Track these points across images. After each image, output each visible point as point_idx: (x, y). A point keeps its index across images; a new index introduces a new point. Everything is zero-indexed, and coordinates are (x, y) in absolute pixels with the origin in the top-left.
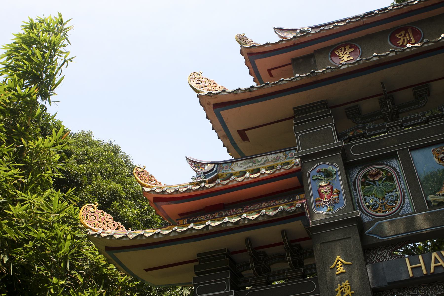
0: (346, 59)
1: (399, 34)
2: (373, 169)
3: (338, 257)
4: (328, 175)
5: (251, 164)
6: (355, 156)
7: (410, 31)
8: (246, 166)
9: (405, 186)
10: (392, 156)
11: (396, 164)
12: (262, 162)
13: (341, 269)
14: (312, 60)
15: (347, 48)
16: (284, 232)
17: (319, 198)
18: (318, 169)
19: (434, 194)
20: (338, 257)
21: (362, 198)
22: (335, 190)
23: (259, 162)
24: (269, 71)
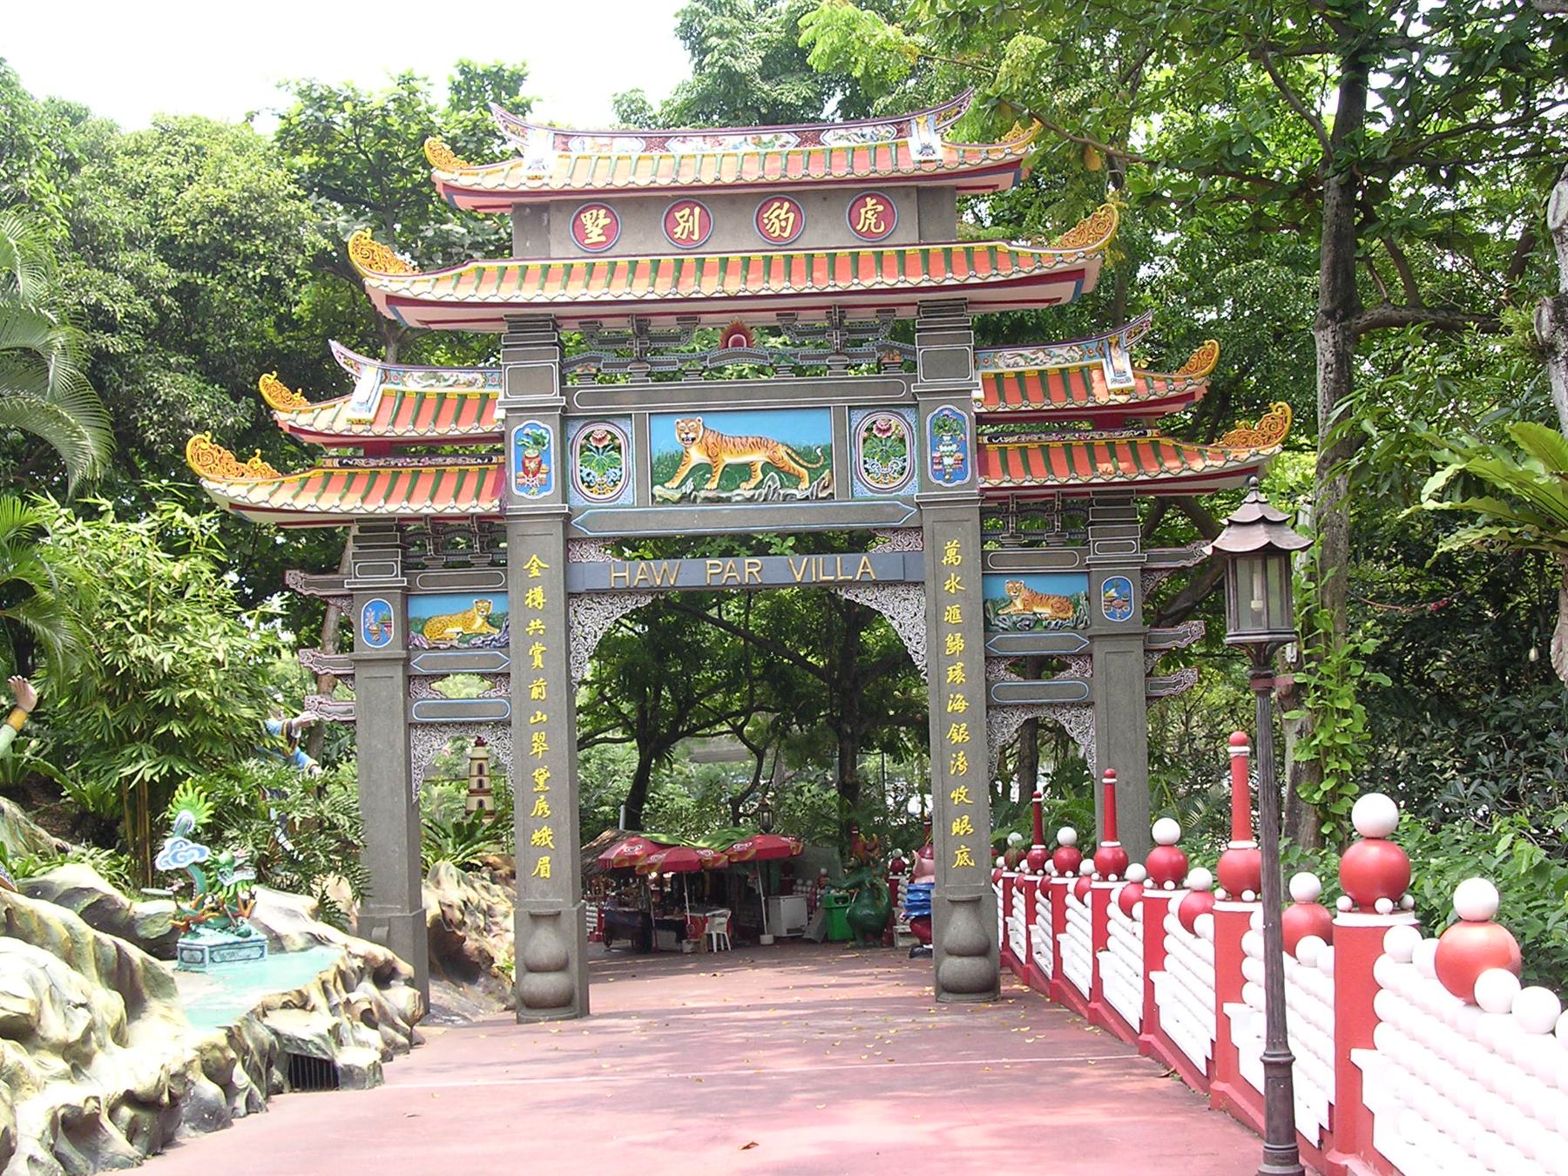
0: (595, 239)
1: (681, 214)
2: (600, 429)
3: (534, 557)
4: (538, 442)
5: (433, 381)
6: (581, 409)
7: (697, 210)
8: (425, 383)
9: (632, 464)
11: (628, 427)
12: (450, 382)
13: (535, 572)
14: (545, 217)
15: (602, 212)
17: (522, 474)
18: (527, 430)
19: (663, 485)
20: (534, 557)
21: (579, 468)
22: (544, 466)
23: (446, 380)
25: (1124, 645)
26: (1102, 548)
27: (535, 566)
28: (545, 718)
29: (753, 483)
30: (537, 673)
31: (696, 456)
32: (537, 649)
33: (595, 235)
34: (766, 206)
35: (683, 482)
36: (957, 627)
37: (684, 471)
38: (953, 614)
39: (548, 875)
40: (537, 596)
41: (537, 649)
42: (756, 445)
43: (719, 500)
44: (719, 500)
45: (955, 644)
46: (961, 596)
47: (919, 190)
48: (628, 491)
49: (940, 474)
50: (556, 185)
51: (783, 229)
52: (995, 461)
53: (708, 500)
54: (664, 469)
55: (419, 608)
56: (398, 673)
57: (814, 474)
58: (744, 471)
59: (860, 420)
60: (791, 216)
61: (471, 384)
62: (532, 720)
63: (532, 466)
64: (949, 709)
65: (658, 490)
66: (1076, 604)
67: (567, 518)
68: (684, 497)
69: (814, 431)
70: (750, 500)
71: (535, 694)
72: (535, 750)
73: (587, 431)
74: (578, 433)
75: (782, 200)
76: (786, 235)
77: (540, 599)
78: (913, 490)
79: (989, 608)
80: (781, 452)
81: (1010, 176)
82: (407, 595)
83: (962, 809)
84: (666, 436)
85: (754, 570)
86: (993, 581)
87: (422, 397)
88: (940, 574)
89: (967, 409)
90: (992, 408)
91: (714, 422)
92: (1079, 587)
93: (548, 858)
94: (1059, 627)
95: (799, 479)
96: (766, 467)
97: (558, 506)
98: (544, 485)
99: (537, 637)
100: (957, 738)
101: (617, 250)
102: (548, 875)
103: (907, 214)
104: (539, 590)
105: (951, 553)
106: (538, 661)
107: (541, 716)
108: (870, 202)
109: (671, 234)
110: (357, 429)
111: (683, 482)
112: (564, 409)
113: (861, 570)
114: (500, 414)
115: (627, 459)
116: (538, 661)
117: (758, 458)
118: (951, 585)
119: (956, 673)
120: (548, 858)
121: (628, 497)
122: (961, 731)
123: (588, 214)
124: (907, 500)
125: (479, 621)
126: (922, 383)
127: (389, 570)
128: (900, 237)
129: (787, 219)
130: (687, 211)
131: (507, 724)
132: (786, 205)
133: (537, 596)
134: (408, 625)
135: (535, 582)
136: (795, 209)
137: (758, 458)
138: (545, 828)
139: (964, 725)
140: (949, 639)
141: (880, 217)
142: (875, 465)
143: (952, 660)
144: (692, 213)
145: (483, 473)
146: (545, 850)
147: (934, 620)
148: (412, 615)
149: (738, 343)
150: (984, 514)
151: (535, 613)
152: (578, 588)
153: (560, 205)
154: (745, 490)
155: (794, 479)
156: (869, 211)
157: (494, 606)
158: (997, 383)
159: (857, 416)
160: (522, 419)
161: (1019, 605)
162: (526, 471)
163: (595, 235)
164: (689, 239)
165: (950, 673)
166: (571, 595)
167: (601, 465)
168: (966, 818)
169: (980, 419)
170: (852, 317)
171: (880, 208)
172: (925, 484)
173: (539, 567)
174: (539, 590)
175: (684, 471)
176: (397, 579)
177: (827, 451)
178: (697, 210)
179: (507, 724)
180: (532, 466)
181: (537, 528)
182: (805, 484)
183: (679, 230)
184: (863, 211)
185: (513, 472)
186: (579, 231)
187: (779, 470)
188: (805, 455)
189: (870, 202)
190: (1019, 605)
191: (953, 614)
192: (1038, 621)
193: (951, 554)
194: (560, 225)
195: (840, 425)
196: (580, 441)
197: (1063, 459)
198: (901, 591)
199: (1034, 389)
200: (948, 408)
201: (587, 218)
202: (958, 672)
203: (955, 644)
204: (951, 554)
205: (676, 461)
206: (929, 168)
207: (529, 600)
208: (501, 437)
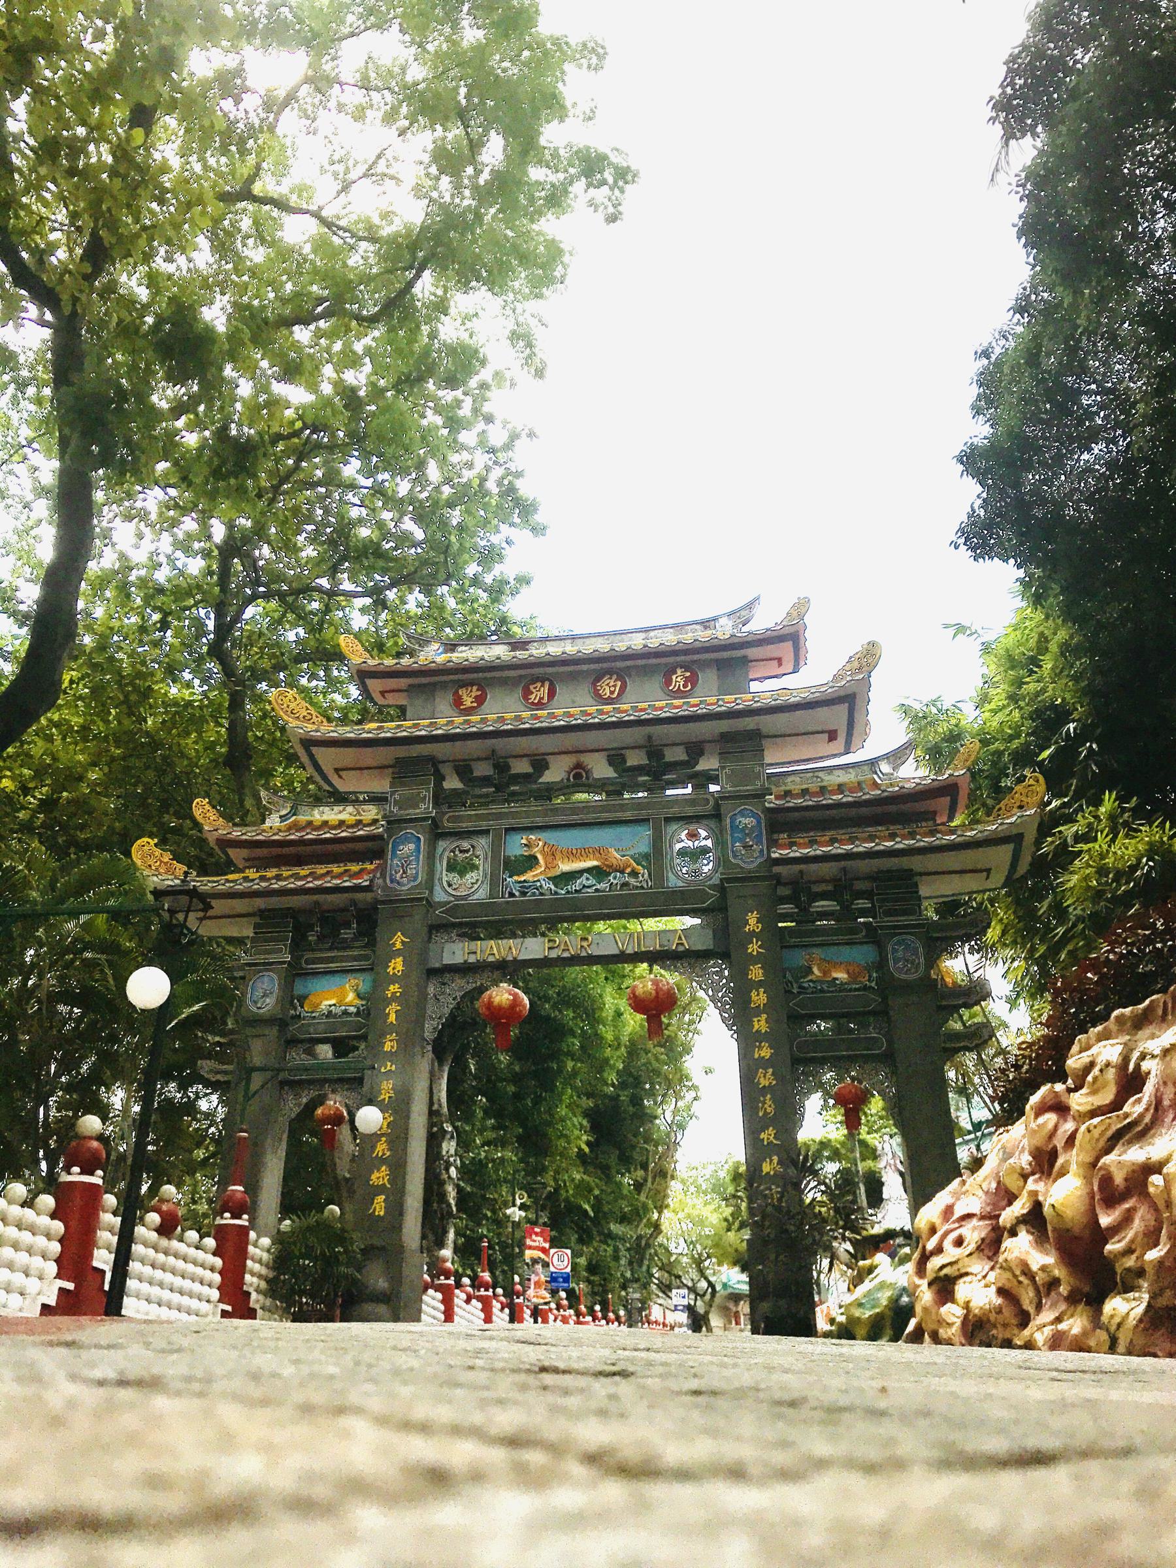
7: (547, 685)
10: (487, 832)
13: (399, 946)
15: (475, 688)
16: (354, 902)
24: (383, 693)
27: (398, 941)
28: (393, 1068)
30: (392, 1028)
34: (598, 679)
36: (760, 984)
38: (756, 973)
39: (382, 1213)
40: (397, 965)
47: (717, 660)
51: (612, 692)
56: (273, 1032)
60: (619, 683)
62: (383, 1070)
64: (756, 1056)
71: (387, 1047)
72: (382, 1097)
76: (615, 695)
77: (400, 968)
85: (585, 944)
93: (384, 1197)
99: (394, 998)
100: (764, 1082)
102: (382, 1213)
104: (400, 960)
106: (392, 1018)
112: (435, 823)
113: (676, 941)
116: (392, 1018)
118: (754, 948)
120: (384, 1197)
122: (768, 1075)
123: (464, 690)
129: (615, 686)
130: (539, 684)
132: (615, 677)
133: (397, 965)
138: (383, 1168)
139: (770, 1070)
140: (753, 994)
141: (687, 680)
143: (758, 1012)
144: (543, 686)
146: (380, 1190)
148: (296, 993)
151: (394, 979)
153: (444, 686)
156: (678, 680)
163: (468, 701)
165: (756, 1024)
168: (775, 1158)
171: (688, 674)
173: (403, 942)
174: (400, 960)
178: (547, 685)
183: (533, 696)
184: (674, 677)
186: (458, 702)
189: (679, 671)
202: (763, 1023)
204: (753, 922)
207: (390, 970)
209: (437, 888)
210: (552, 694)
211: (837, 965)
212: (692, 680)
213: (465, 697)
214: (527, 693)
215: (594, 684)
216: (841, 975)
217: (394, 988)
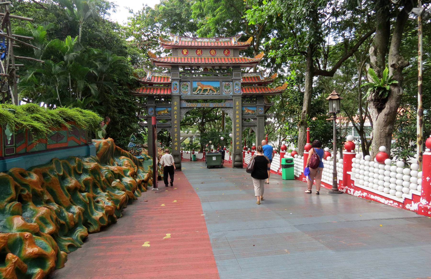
2: (185, 83)
4: (176, 84)
6: (182, 80)
11: (189, 83)
25: (261, 117)
26: (259, 103)
27: (175, 103)
29: (208, 92)
30: (176, 119)
31: (199, 88)
32: (176, 116)
33: (185, 53)
35: (197, 91)
37: (197, 90)
40: (176, 108)
41: (176, 116)
42: (209, 86)
43: (203, 94)
44: (203, 94)
45: (237, 117)
46: (238, 110)
47: (234, 49)
48: (189, 92)
49: (236, 91)
50: (180, 45)
52: (244, 90)
53: (201, 94)
54: (194, 90)
55: (158, 109)
57: (217, 91)
58: (207, 90)
59: (224, 83)
61: (165, 75)
63: (175, 88)
65: (194, 92)
66: (255, 111)
67: (180, 96)
68: (198, 94)
69: (217, 85)
70: (207, 94)
71: (175, 122)
73: (183, 83)
74: (182, 83)
75: (213, 49)
77: (176, 108)
78: (231, 94)
79: (243, 111)
80: (212, 88)
81: (247, 47)
82: (155, 107)
83: (238, 141)
84: (195, 85)
86: (243, 108)
87: (158, 77)
88: (235, 106)
89: (240, 81)
90: (244, 82)
91: (202, 83)
92: (255, 109)
94: (252, 115)
95: (215, 92)
96: (210, 90)
97: (179, 94)
98: (177, 91)
99: (176, 114)
100: (237, 130)
101: (188, 56)
103: (232, 52)
105: (237, 103)
106: (176, 118)
107: (176, 126)
108: (226, 50)
109: (197, 54)
110: (148, 81)
111: (197, 91)
112: (180, 80)
114: (170, 80)
115: (189, 88)
116: (176, 118)
117: (209, 88)
118: (237, 108)
119: (237, 121)
121: (189, 93)
124: (231, 95)
125: (166, 112)
126: (234, 78)
127: (153, 103)
128: (231, 56)
131: (171, 127)
133: (176, 108)
134: (155, 112)
135: (175, 106)
136: (215, 51)
137: (209, 88)
142: (226, 90)
145: (167, 89)
146: (176, 146)
147: (235, 114)
149: (206, 71)
150: (242, 97)
151: (175, 110)
152: (182, 107)
153: (180, 48)
154: (207, 93)
155: (214, 92)
156: (226, 52)
157: (169, 109)
158: (244, 78)
159: (223, 83)
160: (174, 81)
161: (246, 111)
162: (174, 89)
163: (185, 53)
164: (199, 55)
166: (180, 108)
167: (185, 88)
169: (242, 84)
170: (223, 68)
172: (234, 93)
175: (197, 90)
176: (154, 104)
177: (219, 88)
179: (171, 127)
180: (175, 88)
181: (176, 98)
182: (216, 92)
185: (172, 89)
186: (183, 53)
187: (212, 90)
188: (216, 88)
189: (226, 50)
190: (246, 111)
191: (237, 112)
192: (249, 114)
193: (237, 103)
194: (180, 51)
195: (221, 84)
196: (182, 84)
197: (260, 90)
198: (229, 109)
199: (253, 79)
200: (237, 82)
201: (184, 51)
203: (237, 117)
205: (196, 88)
206: (236, 45)
208: (170, 84)
209: (181, 93)
210: (201, 53)
211: (250, 110)
212: (229, 53)
213: (184, 52)
214: (197, 52)
215: (210, 52)
216: (250, 112)
217: (175, 112)
